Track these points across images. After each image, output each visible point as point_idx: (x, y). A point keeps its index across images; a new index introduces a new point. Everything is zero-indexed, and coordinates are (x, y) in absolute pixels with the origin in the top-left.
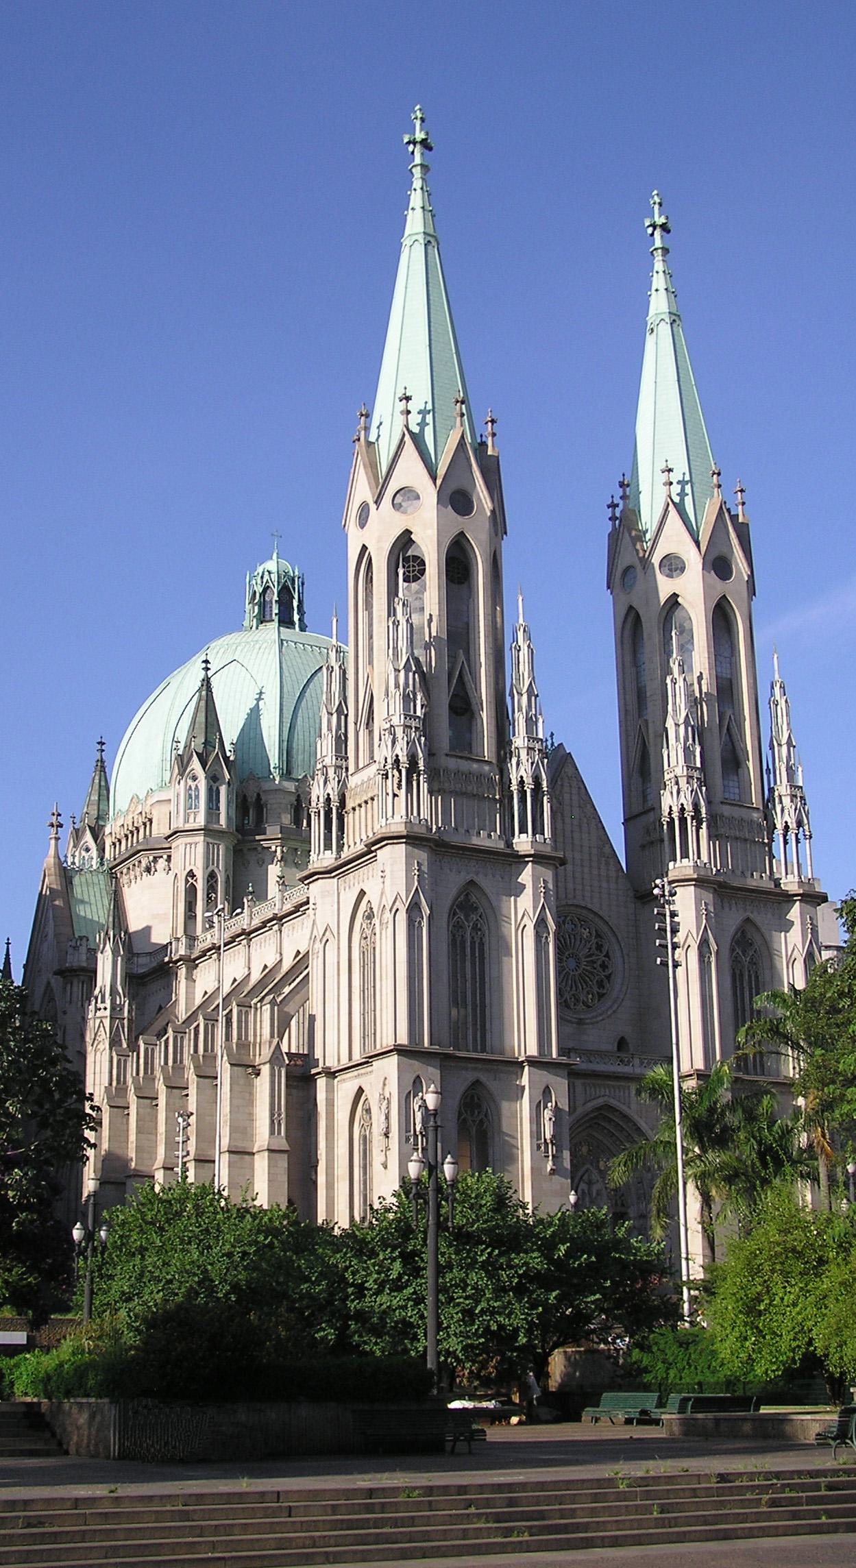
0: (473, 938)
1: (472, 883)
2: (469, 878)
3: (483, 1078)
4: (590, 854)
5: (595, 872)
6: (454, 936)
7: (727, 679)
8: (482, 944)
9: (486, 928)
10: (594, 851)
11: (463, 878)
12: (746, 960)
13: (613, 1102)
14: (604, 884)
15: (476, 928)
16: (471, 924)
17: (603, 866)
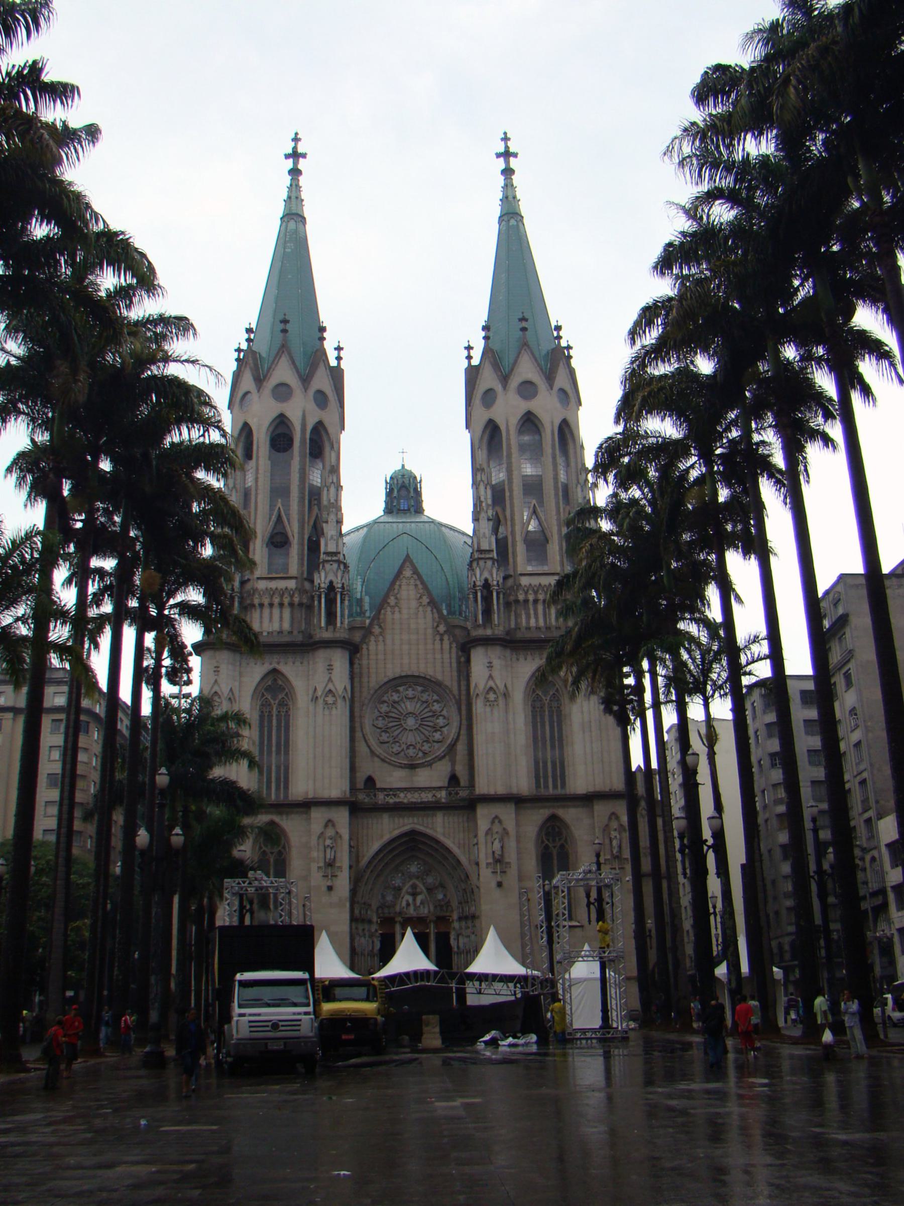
0: (279, 712)
1: (275, 671)
2: (271, 667)
3: (276, 819)
4: (425, 634)
5: (430, 646)
6: (262, 712)
7: (538, 476)
8: (287, 715)
9: (290, 703)
10: (430, 631)
11: (266, 667)
12: (546, 700)
13: (421, 828)
14: (438, 656)
15: (282, 704)
16: (277, 702)
17: (438, 642)
